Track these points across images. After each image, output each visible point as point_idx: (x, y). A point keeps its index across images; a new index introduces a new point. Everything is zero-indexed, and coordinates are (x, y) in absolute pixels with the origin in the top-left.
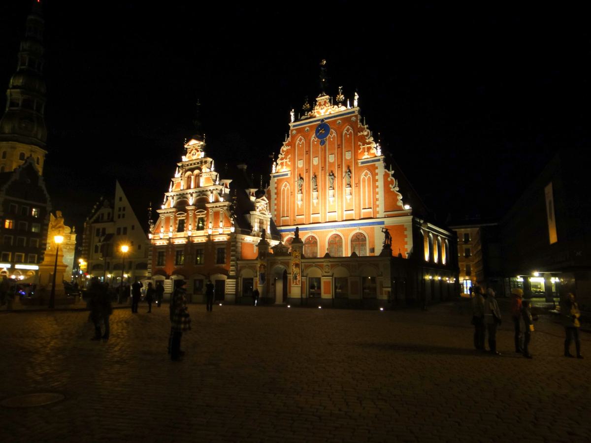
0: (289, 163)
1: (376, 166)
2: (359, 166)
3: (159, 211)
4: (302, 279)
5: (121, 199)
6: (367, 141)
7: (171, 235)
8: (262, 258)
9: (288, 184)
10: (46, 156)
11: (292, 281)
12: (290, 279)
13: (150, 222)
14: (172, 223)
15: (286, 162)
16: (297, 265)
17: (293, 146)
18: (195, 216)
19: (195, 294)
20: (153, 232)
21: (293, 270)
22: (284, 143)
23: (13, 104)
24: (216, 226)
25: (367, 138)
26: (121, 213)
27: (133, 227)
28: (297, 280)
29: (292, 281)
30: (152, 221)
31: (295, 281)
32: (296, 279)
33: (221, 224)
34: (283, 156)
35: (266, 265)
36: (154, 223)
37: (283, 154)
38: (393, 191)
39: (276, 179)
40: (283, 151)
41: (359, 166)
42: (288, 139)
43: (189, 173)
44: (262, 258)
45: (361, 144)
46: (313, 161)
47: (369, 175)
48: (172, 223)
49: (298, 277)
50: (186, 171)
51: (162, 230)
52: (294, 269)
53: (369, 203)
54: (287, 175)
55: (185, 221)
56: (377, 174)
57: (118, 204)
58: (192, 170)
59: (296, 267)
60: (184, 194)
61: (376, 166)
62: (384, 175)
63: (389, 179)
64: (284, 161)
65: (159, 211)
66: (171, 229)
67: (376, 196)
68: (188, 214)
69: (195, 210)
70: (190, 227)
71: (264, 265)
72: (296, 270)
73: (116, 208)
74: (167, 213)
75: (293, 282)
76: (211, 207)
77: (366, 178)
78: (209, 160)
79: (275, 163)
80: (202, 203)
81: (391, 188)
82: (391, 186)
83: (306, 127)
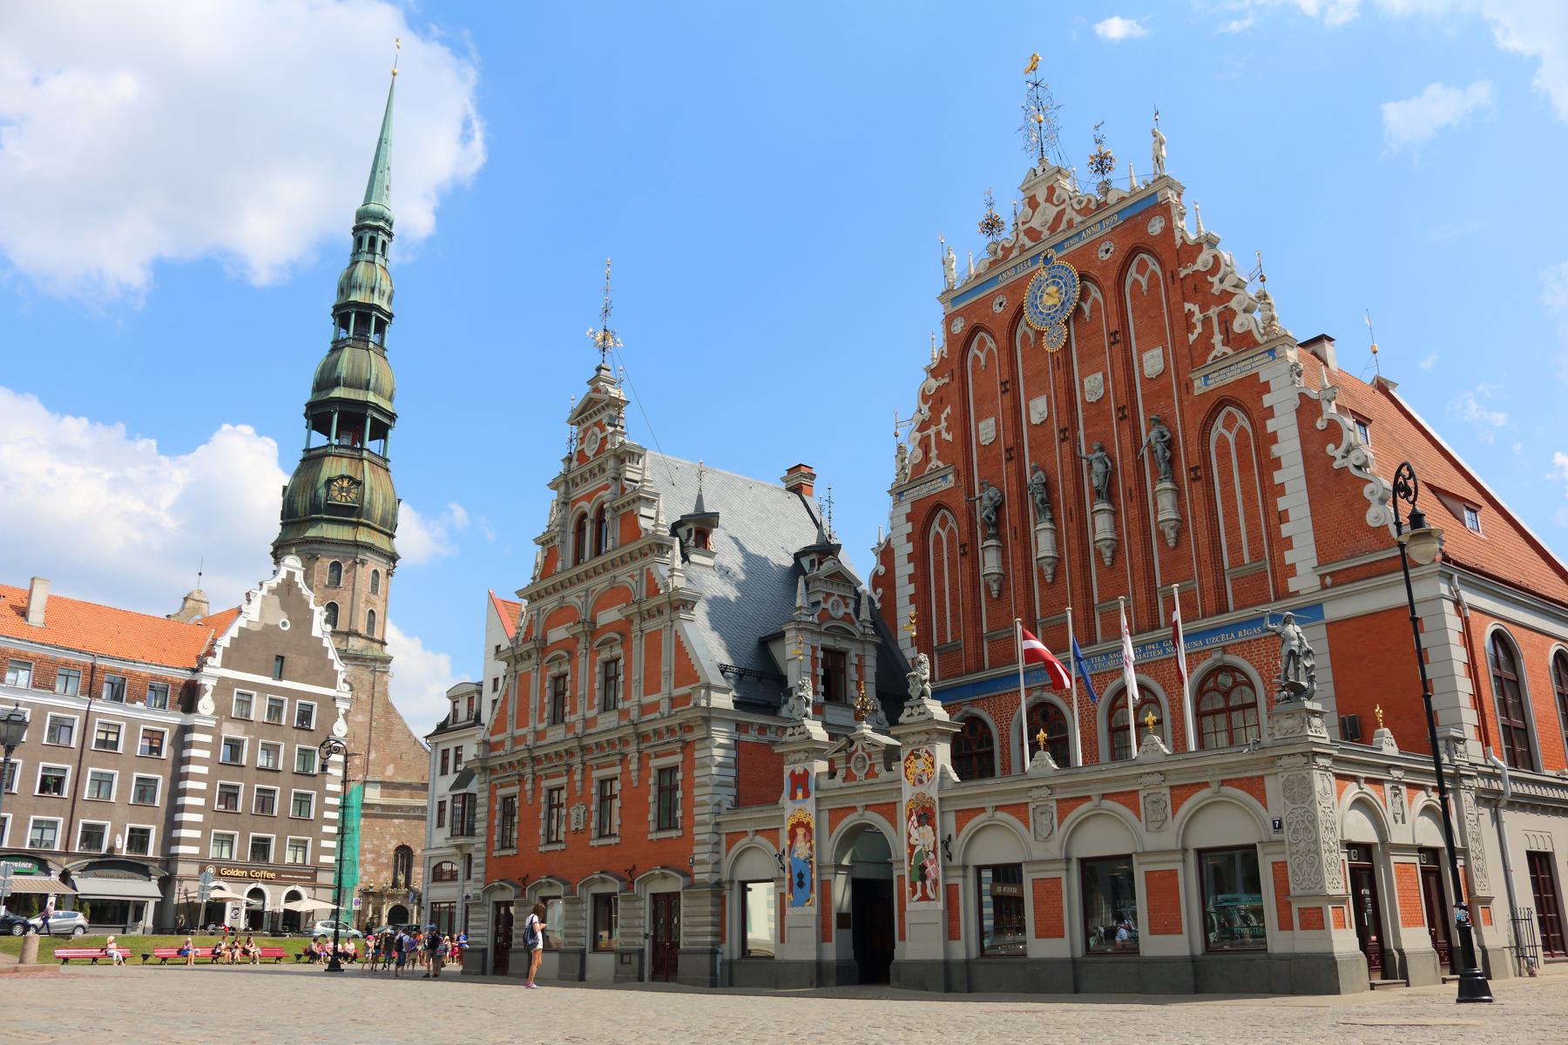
1: (1263, 379)
2: (1196, 393)
4: (945, 877)
6: (1216, 290)
8: (800, 794)
9: (950, 517)
11: (908, 889)
12: (901, 878)
15: (938, 434)
16: (925, 816)
17: (956, 374)
19: (596, 948)
21: (910, 835)
25: (1215, 280)
28: (928, 883)
29: (908, 889)
31: (919, 884)
32: (923, 878)
35: (813, 825)
38: (1343, 470)
41: (1196, 393)
44: (800, 794)
45: (1195, 308)
46: (1028, 415)
47: (1242, 421)
49: (930, 868)
52: (915, 834)
53: (1254, 539)
56: (1270, 413)
59: (920, 824)
61: (1263, 379)
62: (1299, 411)
63: (1320, 424)
64: (932, 431)
67: (1275, 504)
71: (807, 826)
72: (924, 837)
75: (914, 893)
77: (1231, 438)
81: (1334, 458)
82: (1330, 448)
83: (993, 296)
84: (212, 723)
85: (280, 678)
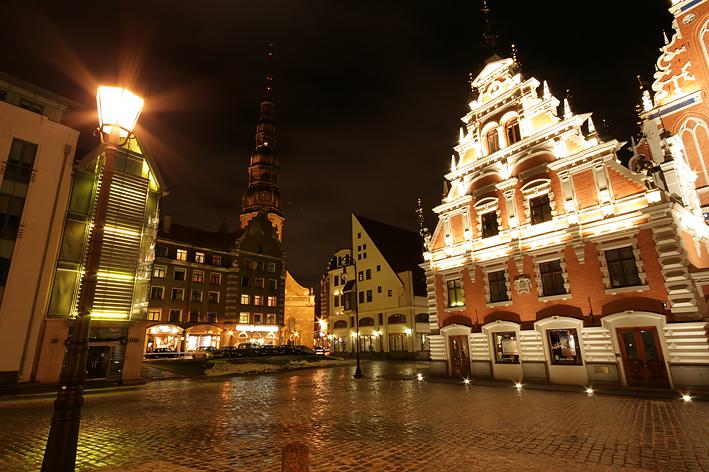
0: (693, 78)
3: (436, 210)
5: (359, 236)
7: (469, 246)
10: (284, 222)
13: (423, 232)
14: (467, 223)
18: (520, 198)
20: (430, 249)
22: (664, 49)
23: (253, 179)
24: (588, 203)
26: (362, 252)
27: (379, 268)
30: (425, 229)
33: (604, 196)
34: (668, 72)
36: (431, 232)
37: (666, 68)
39: (657, 121)
40: (664, 64)
42: (674, 37)
43: (492, 124)
48: (467, 223)
50: (482, 125)
51: (448, 241)
54: (692, 101)
55: (498, 213)
57: (356, 242)
58: (497, 118)
60: (485, 165)
65: (436, 210)
66: (468, 235)
68: (502, 200)
69: (518, 187)
70: (512, 222)
73: (355, 249)
74: (455, 208)
76: (560, 170)
78: (534, 83)
79: (646, 93)
80: (535, 167)
84: (237, 270)
85: (260, 253)
